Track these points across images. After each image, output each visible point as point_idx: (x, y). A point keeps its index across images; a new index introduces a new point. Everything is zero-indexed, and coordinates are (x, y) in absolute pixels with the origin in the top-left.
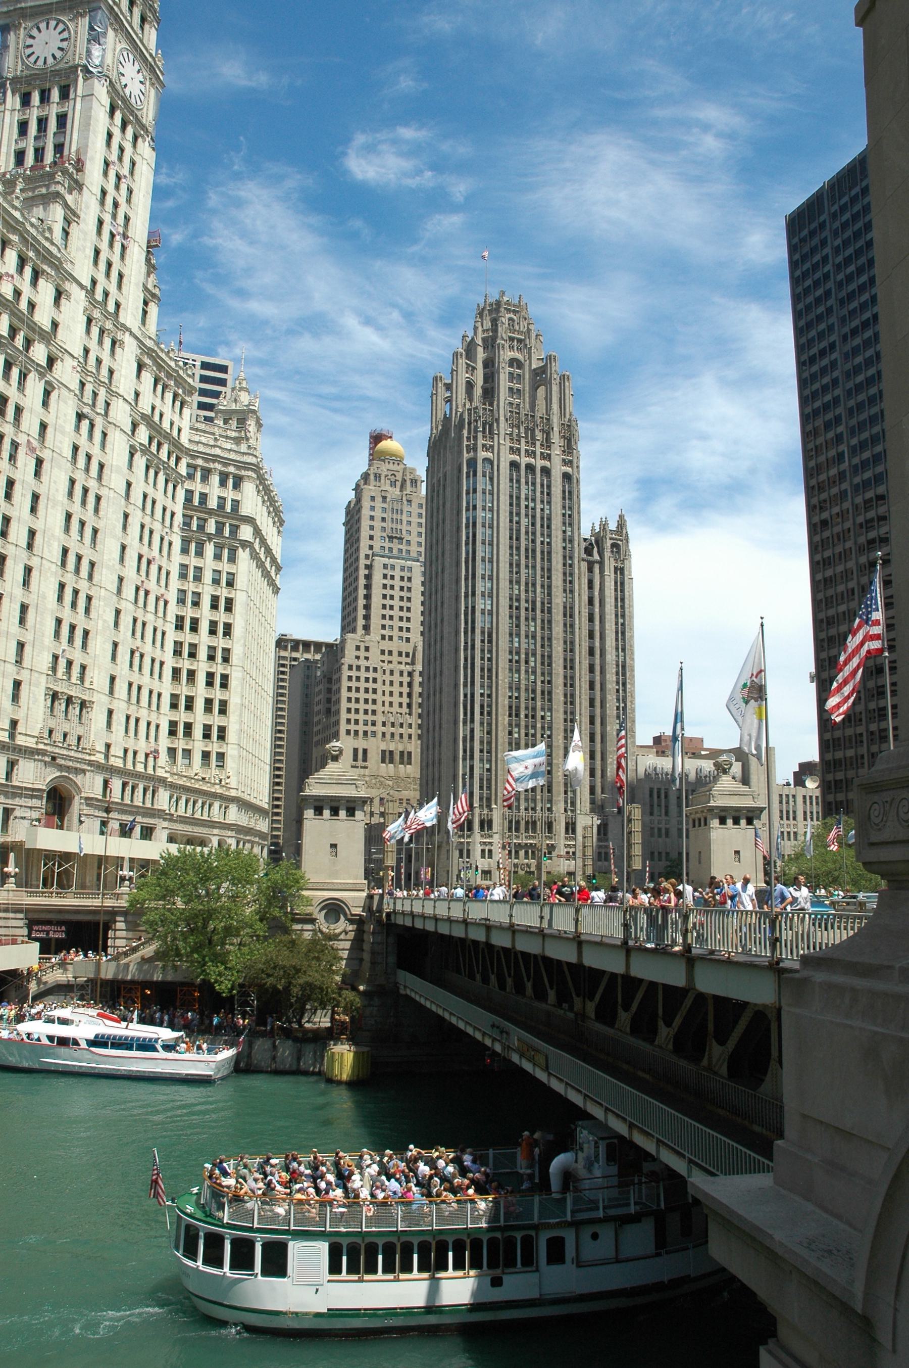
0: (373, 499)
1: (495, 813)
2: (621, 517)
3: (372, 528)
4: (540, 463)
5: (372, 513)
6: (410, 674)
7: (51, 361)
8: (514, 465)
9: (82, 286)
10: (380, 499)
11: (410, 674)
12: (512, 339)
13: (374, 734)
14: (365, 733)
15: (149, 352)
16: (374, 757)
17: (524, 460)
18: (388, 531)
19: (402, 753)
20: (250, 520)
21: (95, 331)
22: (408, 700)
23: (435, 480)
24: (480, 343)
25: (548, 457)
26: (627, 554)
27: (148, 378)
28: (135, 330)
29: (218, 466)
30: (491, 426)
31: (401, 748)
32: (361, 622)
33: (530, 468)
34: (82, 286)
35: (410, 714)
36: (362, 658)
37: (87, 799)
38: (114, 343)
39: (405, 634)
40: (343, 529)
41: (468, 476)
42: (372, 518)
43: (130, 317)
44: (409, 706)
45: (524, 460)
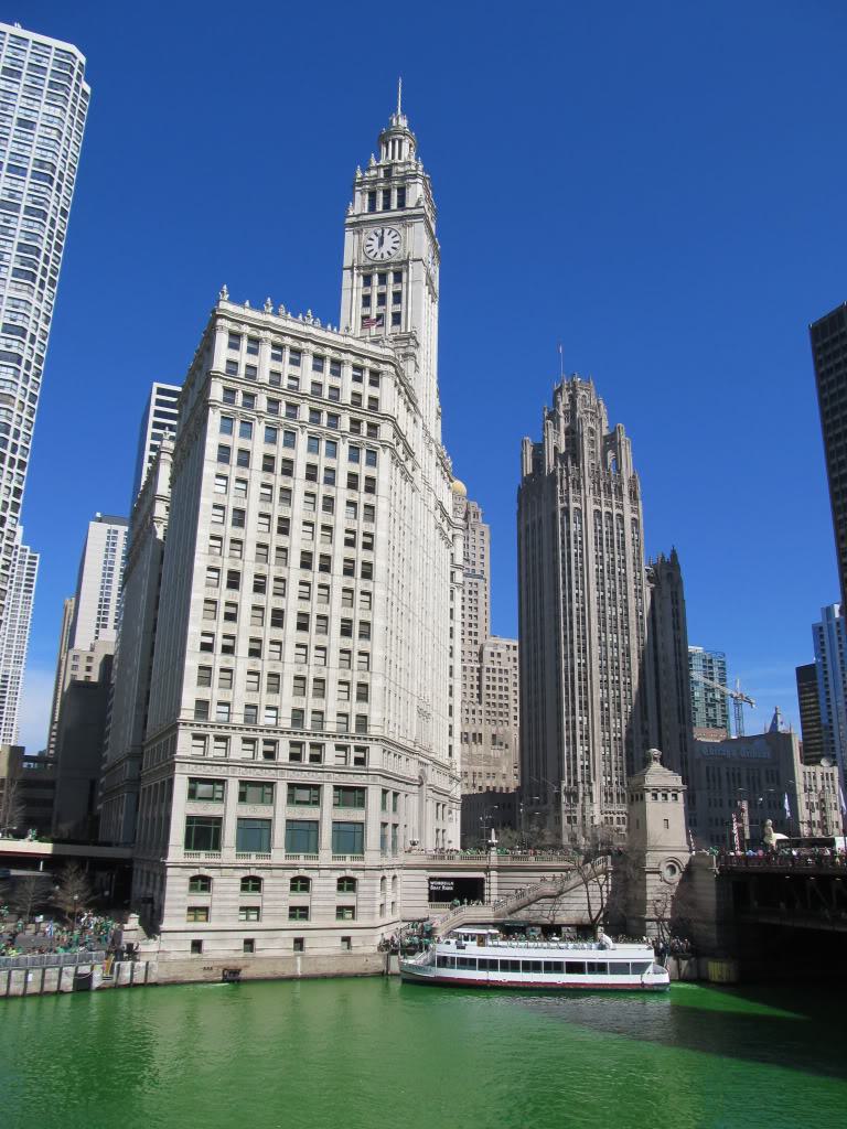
1: (594, 787)
2: (673, 551)
4: (616, 511)
6: (479, 670)
8: (598, 513)
11: (479, 670)
12: (586, 412)
17: (604, 509)
19: (474, 734)
22: (477, 692)
23: (529, 522)
24: (562, 414)
25: (621, 507)
26: (680, 582)
30: (579, 482)
31: (474, 731)
35: (480, 703)
37: (430, 785)
39: (473, 638)
41: (562, 523)
44: (479, 696)
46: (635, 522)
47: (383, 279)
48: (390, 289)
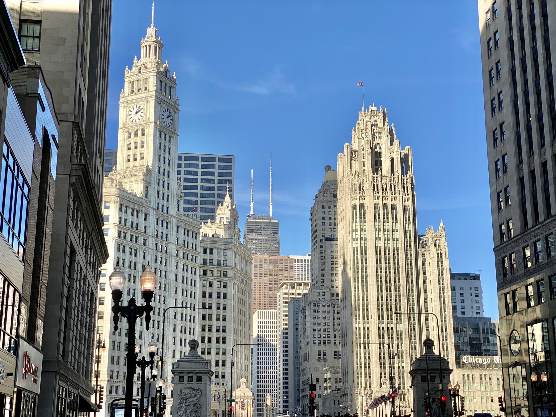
0: (323, 207)
5: (323, 216)
7: (145, 240)
9: (154, 209)
13: (329, 343)
14: (324, 343)
15: (180, 220)
16: (330, 356)
18: (333, 224)
20: (231, 268)
21: (160, 222)
25: (395, 199)
27: (181, 230)
28: (175, 214)
29: (216, 246)
34: (154, 209)
36: (321, 299)
38: (167, 223)
40: (310, 223)
42: (323, 218)
43: (173, 211)
46: (405, 208)
47: (136, 135)
48: (139, 140)
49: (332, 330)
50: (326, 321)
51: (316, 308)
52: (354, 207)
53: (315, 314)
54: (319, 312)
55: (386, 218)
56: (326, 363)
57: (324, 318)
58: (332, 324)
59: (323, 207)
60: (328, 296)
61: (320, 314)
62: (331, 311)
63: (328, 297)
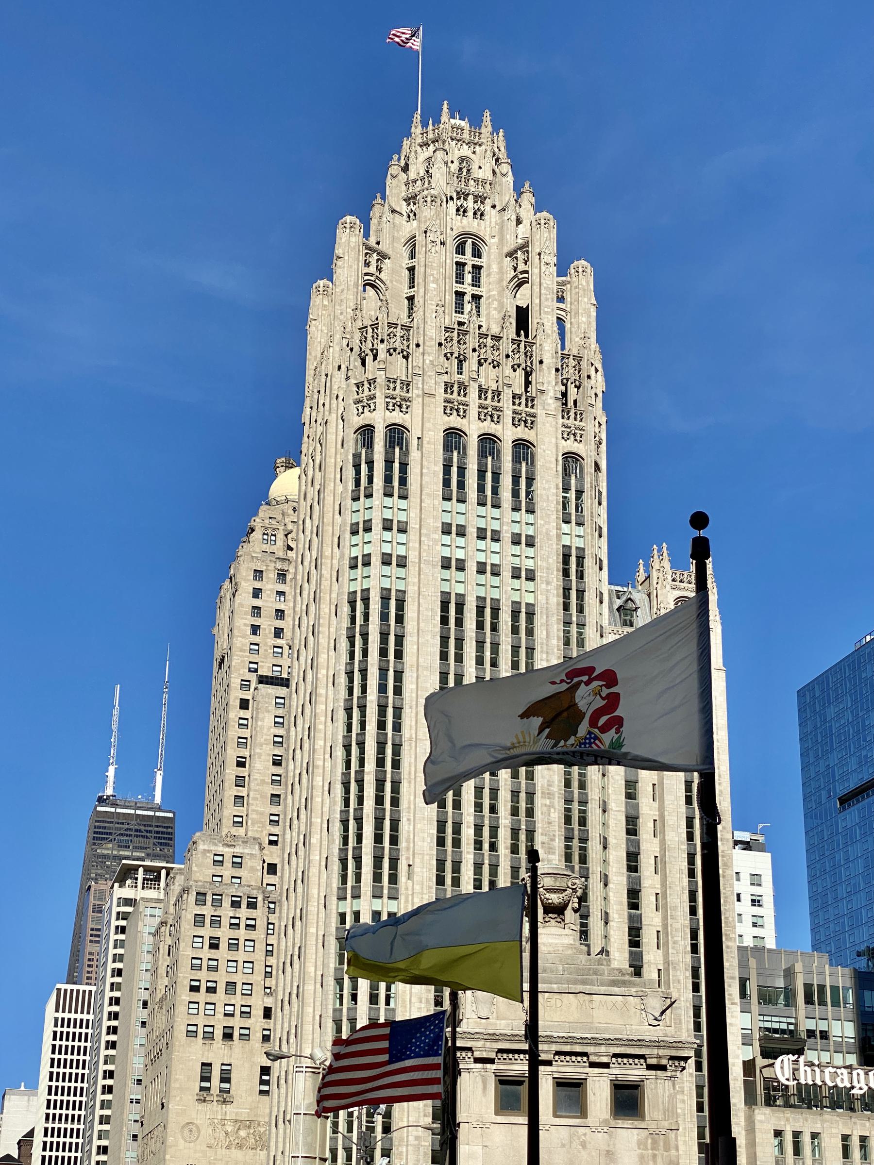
0: (258, 574)
3: (255, 629)
5: (257, 602)
10: (273, 575)
32: (230, 810)
33: (488, 443)
36: (227, 880)
45: (473, 428)
49: (258, 990)
50: (241, 956)
51: (207, 910)
52: (366, 432)
53: (200, 931)
54: (216, 922)
55: (487, 479)
56: (229, 1108)
57: (233, 946)
58: (259, 968)
59: (258, 574)
60: (253, 869)
61: (217, 933)
62: (261, 924)
63: (252, 874)
